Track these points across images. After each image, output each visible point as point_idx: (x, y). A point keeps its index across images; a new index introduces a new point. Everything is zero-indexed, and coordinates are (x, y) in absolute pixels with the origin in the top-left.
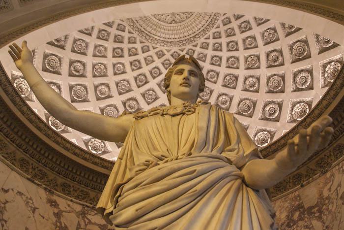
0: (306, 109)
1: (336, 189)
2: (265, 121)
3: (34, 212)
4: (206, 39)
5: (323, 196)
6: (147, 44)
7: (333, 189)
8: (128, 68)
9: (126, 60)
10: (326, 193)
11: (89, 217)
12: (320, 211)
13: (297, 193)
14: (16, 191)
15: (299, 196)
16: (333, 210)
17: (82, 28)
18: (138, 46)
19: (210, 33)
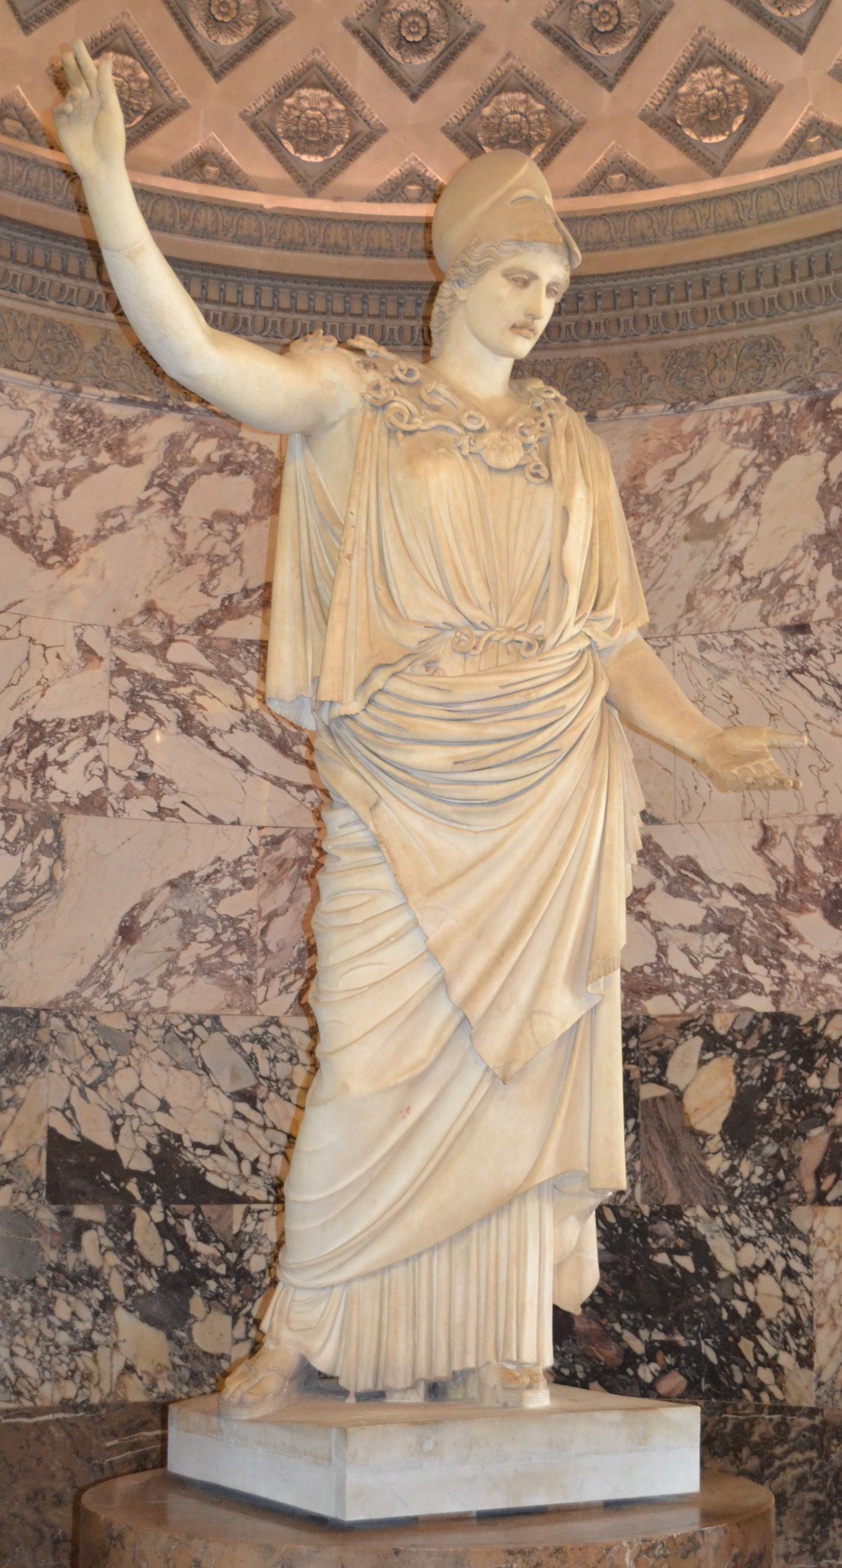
0: (739, 112)
1: (690, 484)
2: (557, 51)
5: (642, 487)
7: (683, 477)
16: (650, 544)
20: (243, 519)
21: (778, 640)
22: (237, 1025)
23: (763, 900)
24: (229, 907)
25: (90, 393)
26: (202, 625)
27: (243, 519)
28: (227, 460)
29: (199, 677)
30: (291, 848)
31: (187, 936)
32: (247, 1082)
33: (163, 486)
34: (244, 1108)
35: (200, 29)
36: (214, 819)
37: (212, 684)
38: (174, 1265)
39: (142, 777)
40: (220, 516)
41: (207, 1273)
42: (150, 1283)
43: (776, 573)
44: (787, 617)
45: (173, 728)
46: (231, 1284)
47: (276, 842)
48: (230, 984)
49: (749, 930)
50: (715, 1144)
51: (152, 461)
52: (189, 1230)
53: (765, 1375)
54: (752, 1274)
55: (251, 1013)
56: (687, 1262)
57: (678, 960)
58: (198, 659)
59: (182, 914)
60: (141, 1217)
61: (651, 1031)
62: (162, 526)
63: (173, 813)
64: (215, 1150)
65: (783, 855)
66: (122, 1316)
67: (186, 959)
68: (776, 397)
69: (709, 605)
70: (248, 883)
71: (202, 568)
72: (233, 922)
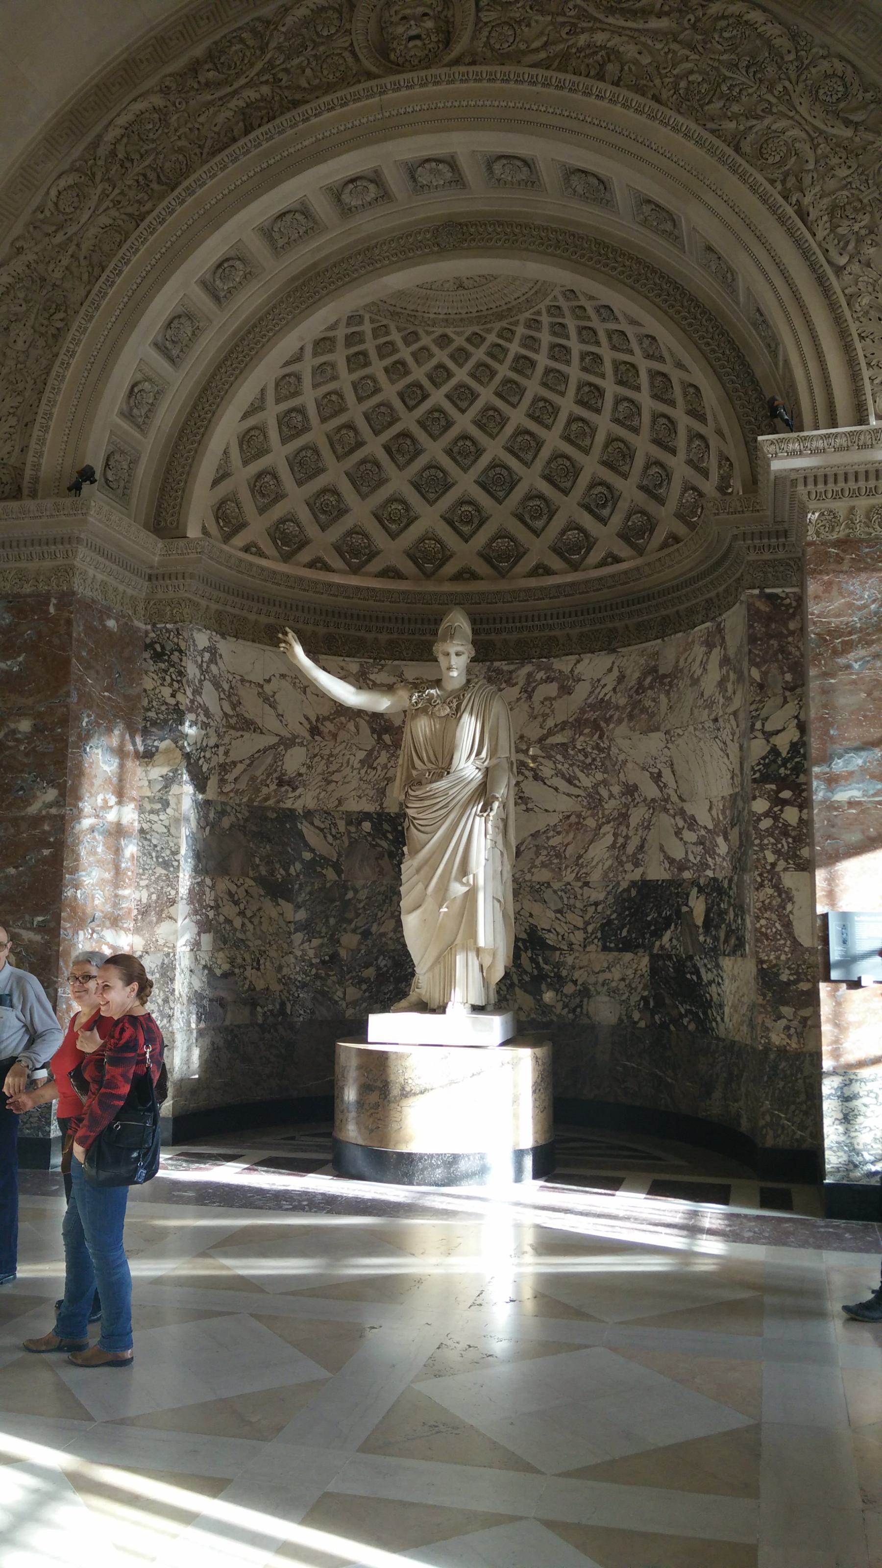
3: (305, 693)
4: (534, 314)
6: (412, 328)
7: (689, 660)
8: (382, 378)
9: (377, 367)
10: (681, 663)
11: (372, 677)
12: (671, 684)
13: (657, 649)
14: (278, 676)
15: (657, 653)
17: (287, 358)
18: (396, 336)
19: (542, 306)
20: (554, 699)
21: (711, 725)
22: (556, 886)
23: (709, 831)
24: (552, 842)
25: (497, 664)
26: (541, 740)
27: (554, 699)
28: (548, 678)
29: (540, 759)
30: (573, 819)
31: (538, 854)
32: (560, 906)
33: (526, 691)
34: (559, 915)
35: (528, 520)
36: (546, 811)
37: (545, 762)
38: (536, 972)
39: (520, 798)
40: (546, 699)
41: (547, 976)
42: (527, 978)
43: (711, 697)
44: (713, 717)
45: (531, 779)
46: (555, 980)
47: (568, 817)
48: (553, 870)
49: (708, 844)
50: (701, 930)
51: (521, 684)
52: (540, 959)
53: (714, 1024)
54: (710, 983)
55: (560, 880)
56: (694, 977)
57: (691, 857)
58: (539, 752)
59: (537, 846)
60: (523, 955)
61: (685, 884)
62: (525, 706)
63: (532, 809)
64: (549, 931)
65: (714, 812)
66: (517, 990)
67: (537, 862)
68: (708, 624)
69: (696, 711)
70: (559, 833)
71: (540, 719)
72: (554, 847)
